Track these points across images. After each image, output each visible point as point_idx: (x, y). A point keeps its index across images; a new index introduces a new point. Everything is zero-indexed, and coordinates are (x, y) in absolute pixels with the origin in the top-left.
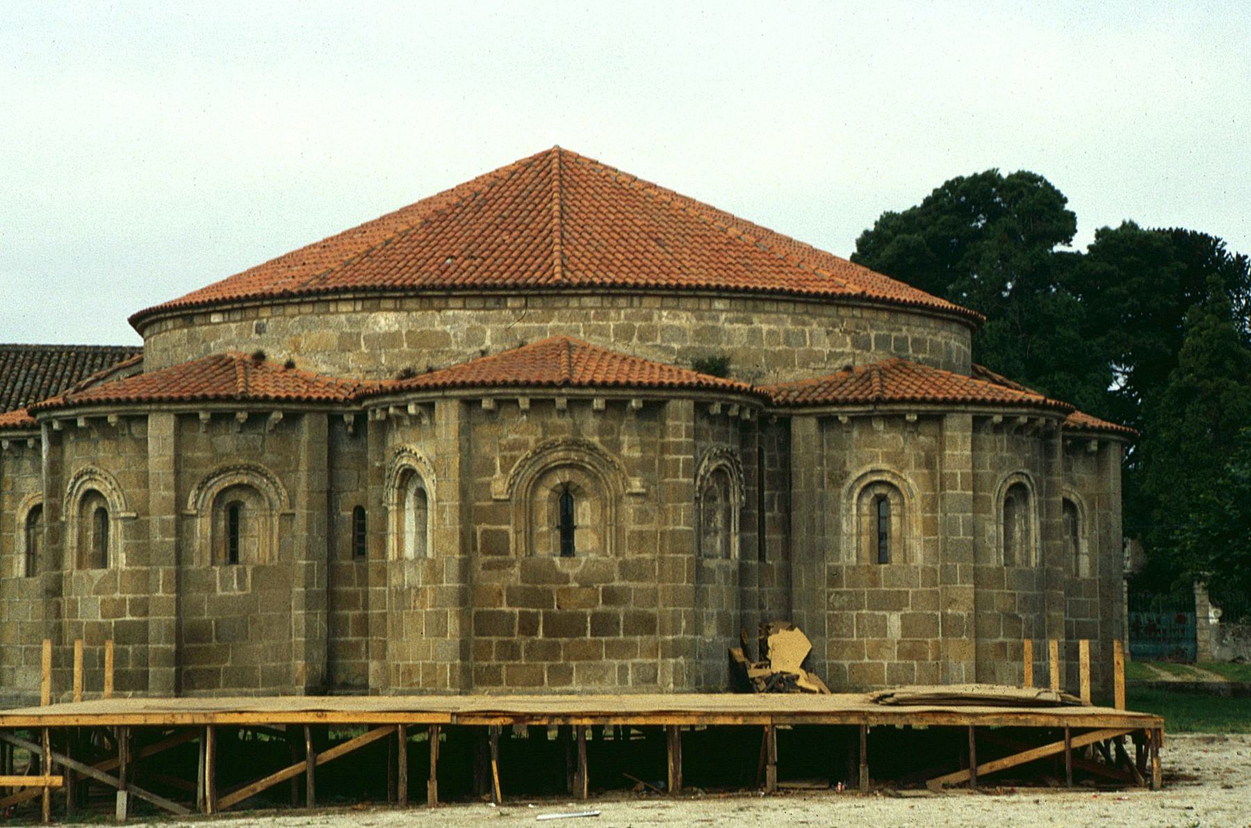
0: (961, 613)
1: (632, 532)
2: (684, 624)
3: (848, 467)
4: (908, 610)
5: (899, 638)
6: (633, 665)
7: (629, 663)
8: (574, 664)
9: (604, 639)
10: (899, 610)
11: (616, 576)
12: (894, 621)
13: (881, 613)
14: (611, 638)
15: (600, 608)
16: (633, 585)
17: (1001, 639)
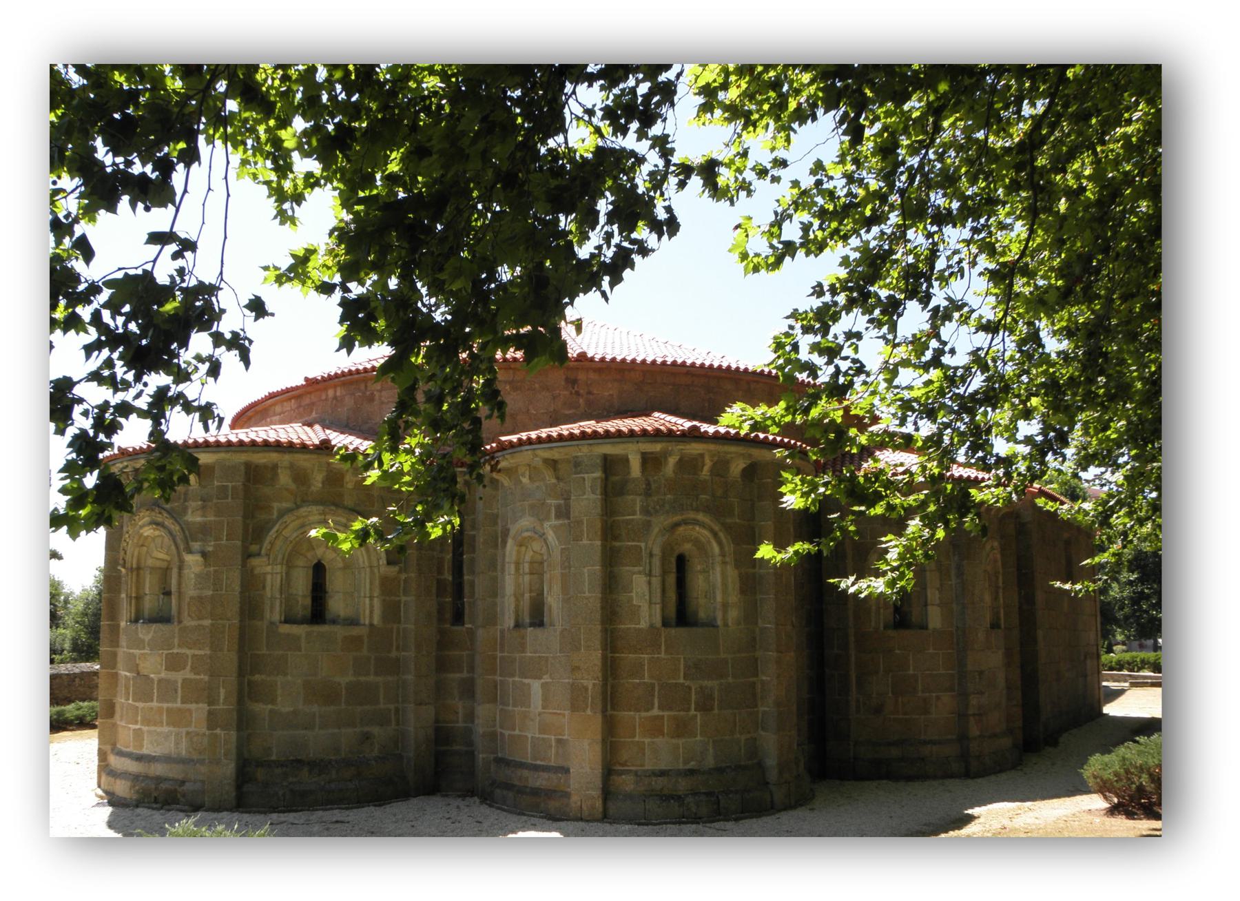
0: (585, 682)
1: (191, 598)
2: (222, 697)
3: (509, 526)
4: (546, 678)
5: (540, 709)
6: (188, 733)
7: (184, 730)
8: (145, 728)
9: (165, 705)
10: (540, 678)
11: (176, 641)
12: (536, 686)
13: (526, 681)
14: (170, 705)
15: (163, 675)
16: (189, 652)
17: (656, 712)
